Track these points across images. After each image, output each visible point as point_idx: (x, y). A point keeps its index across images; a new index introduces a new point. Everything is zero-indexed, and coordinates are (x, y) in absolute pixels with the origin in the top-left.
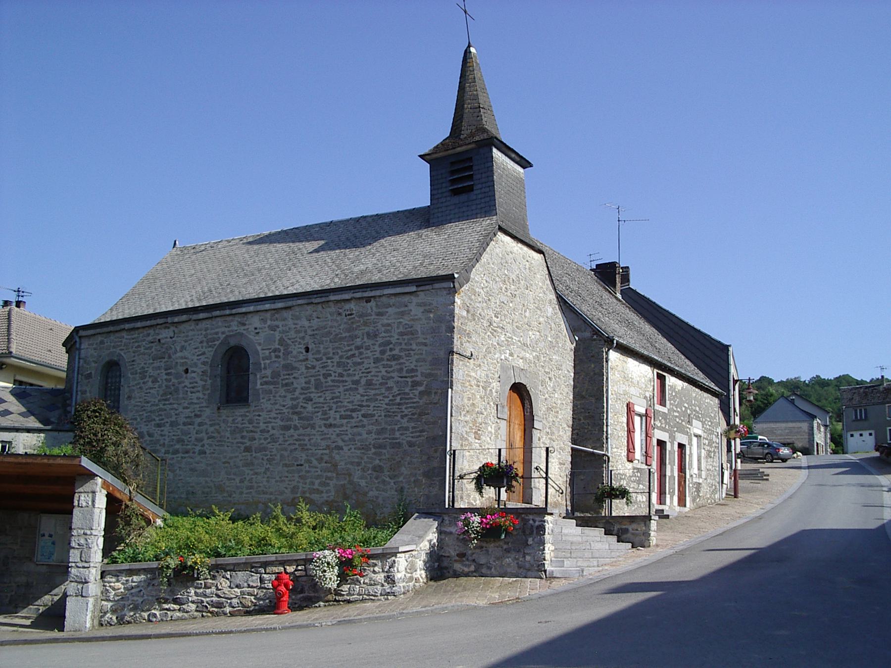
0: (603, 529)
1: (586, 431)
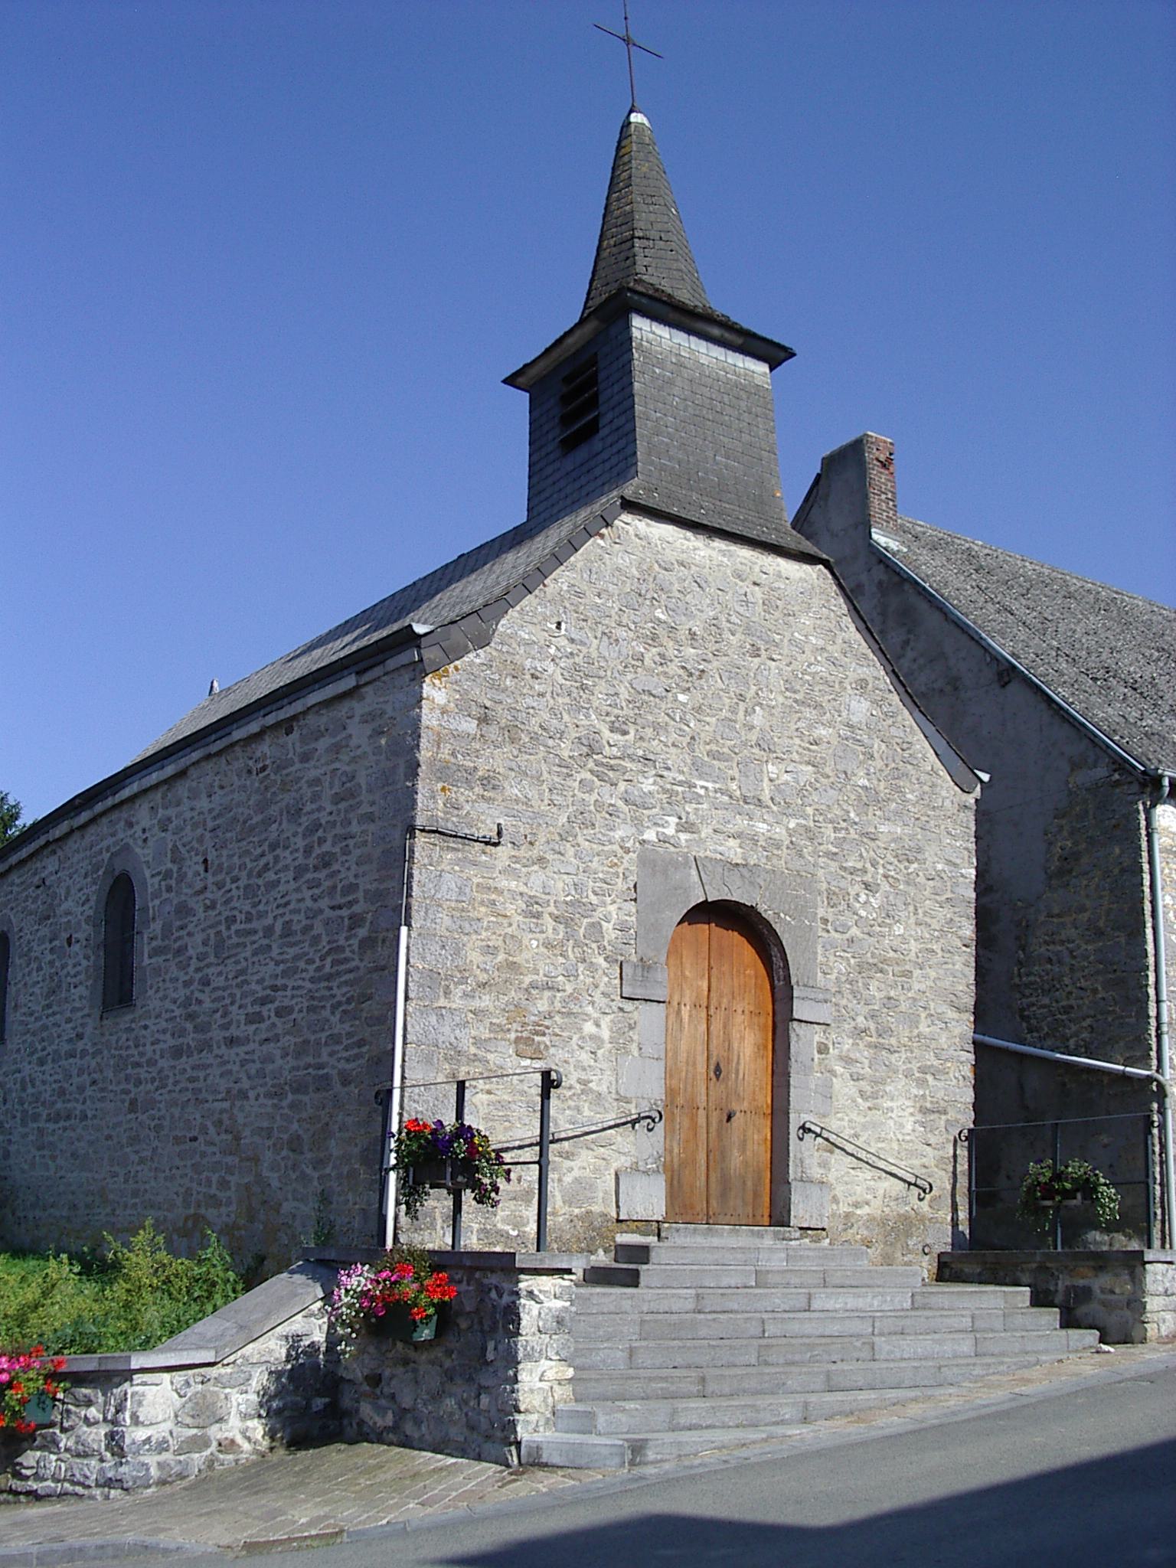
0: (1028, 1289)
1: (1110, 1019)
